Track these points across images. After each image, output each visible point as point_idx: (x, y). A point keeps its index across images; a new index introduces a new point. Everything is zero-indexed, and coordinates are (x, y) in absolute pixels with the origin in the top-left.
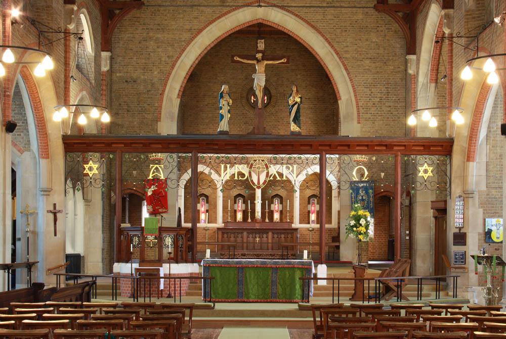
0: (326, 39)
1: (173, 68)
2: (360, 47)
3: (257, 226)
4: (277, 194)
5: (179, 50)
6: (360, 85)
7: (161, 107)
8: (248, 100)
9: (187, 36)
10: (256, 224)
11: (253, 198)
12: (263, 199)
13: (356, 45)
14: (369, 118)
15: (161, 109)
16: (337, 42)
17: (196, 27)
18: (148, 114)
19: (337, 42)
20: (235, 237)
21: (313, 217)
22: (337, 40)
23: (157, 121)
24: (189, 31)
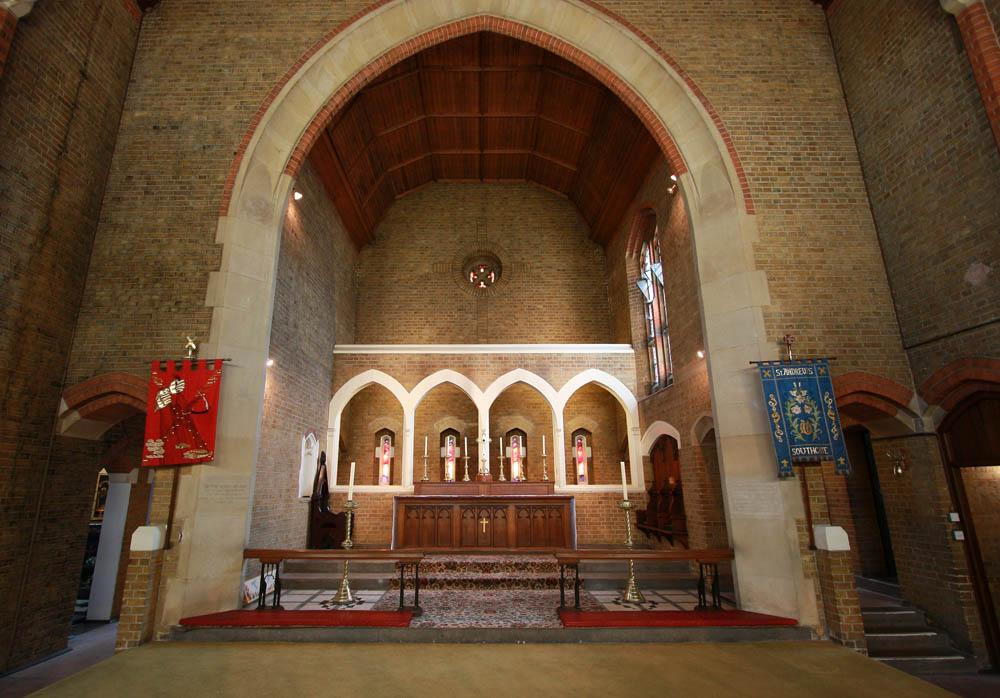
0: (643, 36)
1: (273, 98)
2: (723, 50)
3: (483, 492)
4: (517, 429)
5: (291, 61)
6: (736, 128)
7: (233, 182)
8: (467, 278)
9: (311, 34)
10: (481, 486)
11: (474, 433)
12: (491, 435)
13: (715, 46)
14: (775, 202)
15: (232, 188)
16: (668, 41)
17: (335, 18)
18: (199, 198)
19: (668, 41)
20: (434, 517)
21: (582, 469)
22: (668, 37)
23: (218, 215)
24: (319, 25)
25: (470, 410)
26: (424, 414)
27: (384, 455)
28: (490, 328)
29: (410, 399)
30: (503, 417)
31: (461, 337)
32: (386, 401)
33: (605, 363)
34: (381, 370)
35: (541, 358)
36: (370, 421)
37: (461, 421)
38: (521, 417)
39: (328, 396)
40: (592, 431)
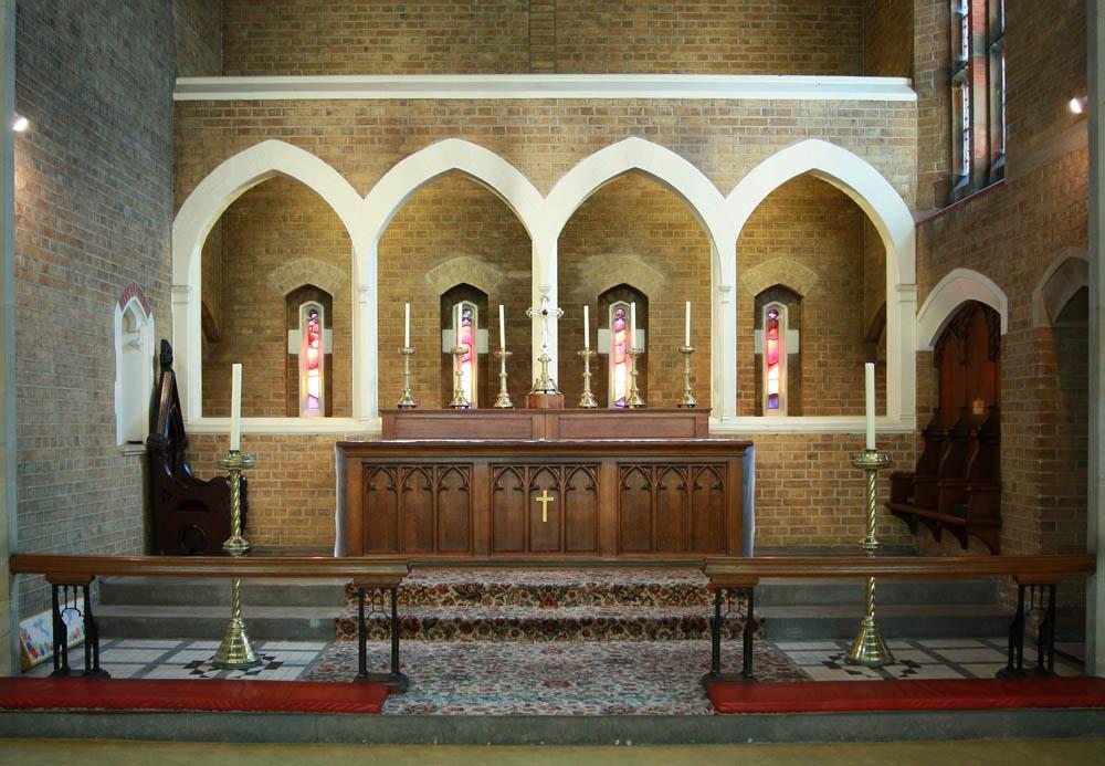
4: (624, 287)
10: (538, 419)
11: (520, 297)
12: (564, 299)
20: (429, 489)
21: (775, 381)
25: (513, 242)
26: (404, 245)
27: (309, 347)
28: (563, 33)
29: (364, 211)
30: (592, 258)
31: (488, 56)
32: (309, 219)
33: (845, 126)
34: (293, 142)
35: (687, 109)
36: (271, 268)
37: (492, 268)
38: (634, 258)
39: (166, 207)
40: (804, 292)
